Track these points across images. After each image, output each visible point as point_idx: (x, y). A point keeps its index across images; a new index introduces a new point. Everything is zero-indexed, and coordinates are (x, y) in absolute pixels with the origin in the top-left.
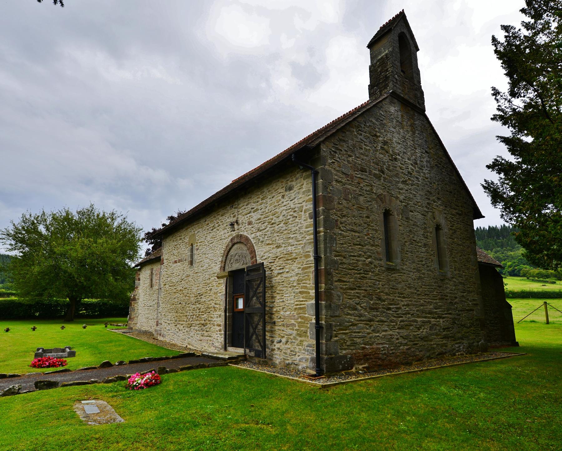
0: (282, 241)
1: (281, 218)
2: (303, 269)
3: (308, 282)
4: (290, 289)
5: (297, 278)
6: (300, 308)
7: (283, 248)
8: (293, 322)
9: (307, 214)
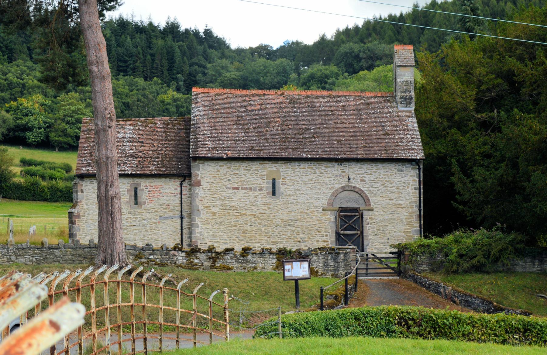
0: (394, 197)
1: (394, 184)
2: (410, 213)
3: (412, 219)
4: (400, 222)
5: (405, 217)
6: (407, 232)
7: (394, 201)
8: (402, 238)
9: (413, 187)
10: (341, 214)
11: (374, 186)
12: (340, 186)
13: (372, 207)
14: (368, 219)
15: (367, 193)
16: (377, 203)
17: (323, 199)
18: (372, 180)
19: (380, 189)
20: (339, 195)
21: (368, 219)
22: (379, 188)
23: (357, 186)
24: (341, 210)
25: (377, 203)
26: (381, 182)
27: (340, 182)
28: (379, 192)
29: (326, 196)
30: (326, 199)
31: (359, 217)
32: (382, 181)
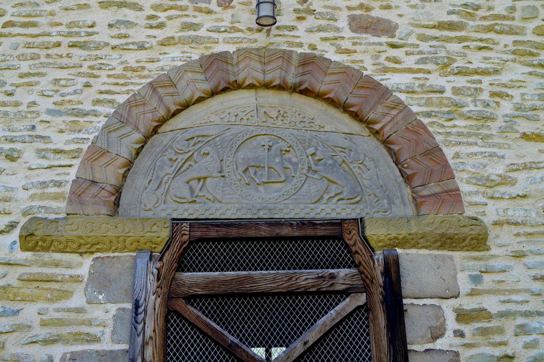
10: (188, 277)
11: (460, 63)
12: (196, 57)
13: (470, 212)
14: (451, 324)
15: (415, 109)
16: (505, 181)
17: (41, 154)
18: (440, 26)
19: (514, 84)
20: (179, 122)
21: (451, 324)
22: (505, 78)
23: (332, 56)
24: (194, 242)
25: (505, 181)
26: (508, 39)
27: (202, 32)
28: (507, 107)
29: (75, 128)
30: (74, 154)
31: (366, 308)
32: (511, 32)
